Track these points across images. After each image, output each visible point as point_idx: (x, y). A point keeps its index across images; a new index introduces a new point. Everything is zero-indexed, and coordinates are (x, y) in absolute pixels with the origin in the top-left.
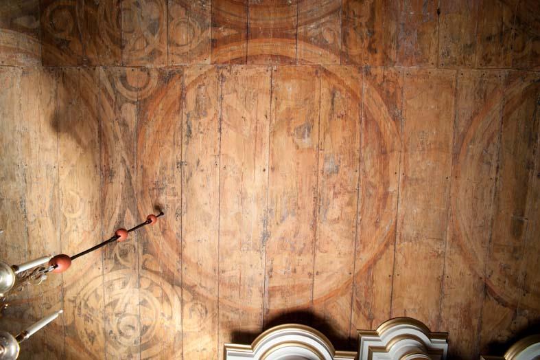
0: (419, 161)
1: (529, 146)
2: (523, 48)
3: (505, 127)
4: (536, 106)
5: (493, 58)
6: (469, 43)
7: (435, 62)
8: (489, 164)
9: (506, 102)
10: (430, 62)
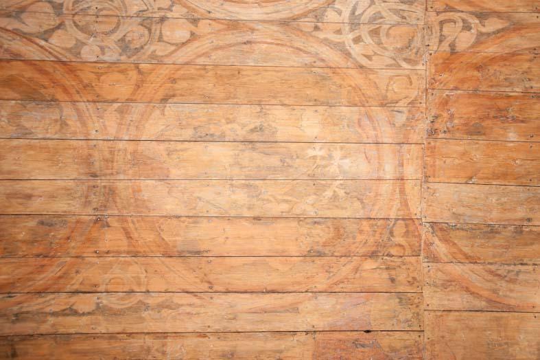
0: (520, 348)
1: (499, 233)
2: (400, 246)
3: (479, 259)
4: (458, 229)
5: (411, 275)
6: (398, 300)
7: (417, 334)
8: (518, 273)
9: (454, 260)
10: (418, 339)
